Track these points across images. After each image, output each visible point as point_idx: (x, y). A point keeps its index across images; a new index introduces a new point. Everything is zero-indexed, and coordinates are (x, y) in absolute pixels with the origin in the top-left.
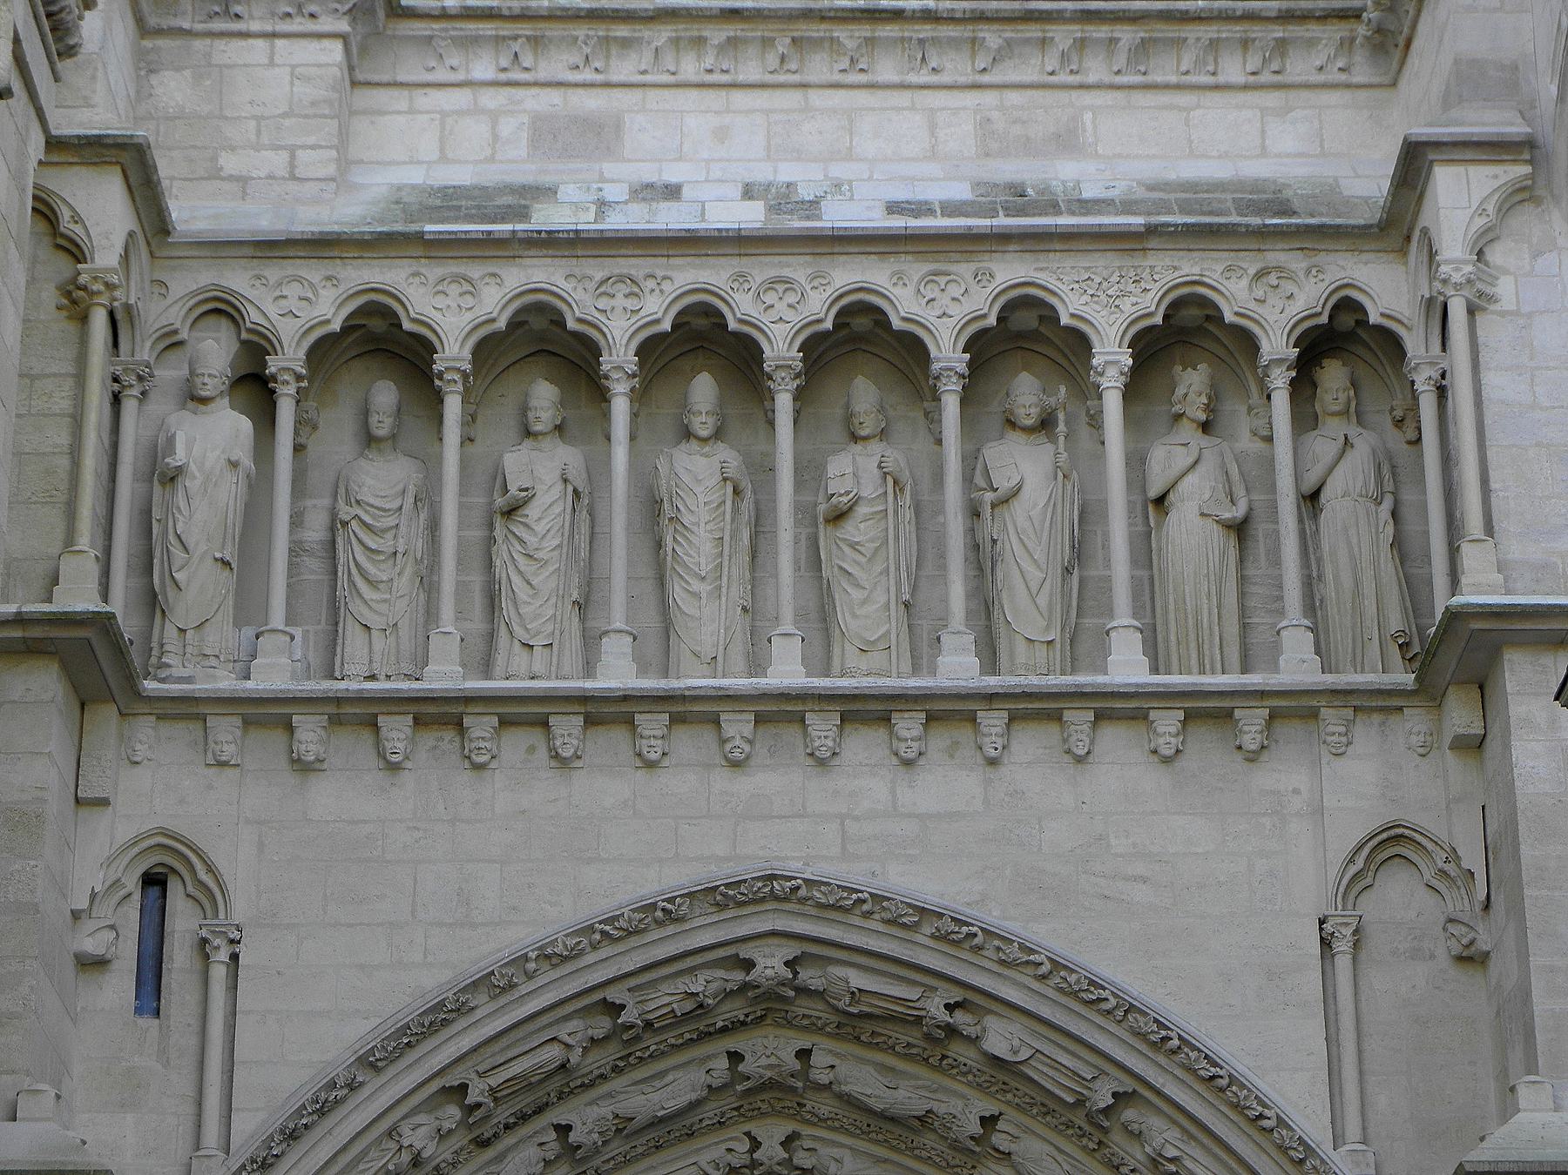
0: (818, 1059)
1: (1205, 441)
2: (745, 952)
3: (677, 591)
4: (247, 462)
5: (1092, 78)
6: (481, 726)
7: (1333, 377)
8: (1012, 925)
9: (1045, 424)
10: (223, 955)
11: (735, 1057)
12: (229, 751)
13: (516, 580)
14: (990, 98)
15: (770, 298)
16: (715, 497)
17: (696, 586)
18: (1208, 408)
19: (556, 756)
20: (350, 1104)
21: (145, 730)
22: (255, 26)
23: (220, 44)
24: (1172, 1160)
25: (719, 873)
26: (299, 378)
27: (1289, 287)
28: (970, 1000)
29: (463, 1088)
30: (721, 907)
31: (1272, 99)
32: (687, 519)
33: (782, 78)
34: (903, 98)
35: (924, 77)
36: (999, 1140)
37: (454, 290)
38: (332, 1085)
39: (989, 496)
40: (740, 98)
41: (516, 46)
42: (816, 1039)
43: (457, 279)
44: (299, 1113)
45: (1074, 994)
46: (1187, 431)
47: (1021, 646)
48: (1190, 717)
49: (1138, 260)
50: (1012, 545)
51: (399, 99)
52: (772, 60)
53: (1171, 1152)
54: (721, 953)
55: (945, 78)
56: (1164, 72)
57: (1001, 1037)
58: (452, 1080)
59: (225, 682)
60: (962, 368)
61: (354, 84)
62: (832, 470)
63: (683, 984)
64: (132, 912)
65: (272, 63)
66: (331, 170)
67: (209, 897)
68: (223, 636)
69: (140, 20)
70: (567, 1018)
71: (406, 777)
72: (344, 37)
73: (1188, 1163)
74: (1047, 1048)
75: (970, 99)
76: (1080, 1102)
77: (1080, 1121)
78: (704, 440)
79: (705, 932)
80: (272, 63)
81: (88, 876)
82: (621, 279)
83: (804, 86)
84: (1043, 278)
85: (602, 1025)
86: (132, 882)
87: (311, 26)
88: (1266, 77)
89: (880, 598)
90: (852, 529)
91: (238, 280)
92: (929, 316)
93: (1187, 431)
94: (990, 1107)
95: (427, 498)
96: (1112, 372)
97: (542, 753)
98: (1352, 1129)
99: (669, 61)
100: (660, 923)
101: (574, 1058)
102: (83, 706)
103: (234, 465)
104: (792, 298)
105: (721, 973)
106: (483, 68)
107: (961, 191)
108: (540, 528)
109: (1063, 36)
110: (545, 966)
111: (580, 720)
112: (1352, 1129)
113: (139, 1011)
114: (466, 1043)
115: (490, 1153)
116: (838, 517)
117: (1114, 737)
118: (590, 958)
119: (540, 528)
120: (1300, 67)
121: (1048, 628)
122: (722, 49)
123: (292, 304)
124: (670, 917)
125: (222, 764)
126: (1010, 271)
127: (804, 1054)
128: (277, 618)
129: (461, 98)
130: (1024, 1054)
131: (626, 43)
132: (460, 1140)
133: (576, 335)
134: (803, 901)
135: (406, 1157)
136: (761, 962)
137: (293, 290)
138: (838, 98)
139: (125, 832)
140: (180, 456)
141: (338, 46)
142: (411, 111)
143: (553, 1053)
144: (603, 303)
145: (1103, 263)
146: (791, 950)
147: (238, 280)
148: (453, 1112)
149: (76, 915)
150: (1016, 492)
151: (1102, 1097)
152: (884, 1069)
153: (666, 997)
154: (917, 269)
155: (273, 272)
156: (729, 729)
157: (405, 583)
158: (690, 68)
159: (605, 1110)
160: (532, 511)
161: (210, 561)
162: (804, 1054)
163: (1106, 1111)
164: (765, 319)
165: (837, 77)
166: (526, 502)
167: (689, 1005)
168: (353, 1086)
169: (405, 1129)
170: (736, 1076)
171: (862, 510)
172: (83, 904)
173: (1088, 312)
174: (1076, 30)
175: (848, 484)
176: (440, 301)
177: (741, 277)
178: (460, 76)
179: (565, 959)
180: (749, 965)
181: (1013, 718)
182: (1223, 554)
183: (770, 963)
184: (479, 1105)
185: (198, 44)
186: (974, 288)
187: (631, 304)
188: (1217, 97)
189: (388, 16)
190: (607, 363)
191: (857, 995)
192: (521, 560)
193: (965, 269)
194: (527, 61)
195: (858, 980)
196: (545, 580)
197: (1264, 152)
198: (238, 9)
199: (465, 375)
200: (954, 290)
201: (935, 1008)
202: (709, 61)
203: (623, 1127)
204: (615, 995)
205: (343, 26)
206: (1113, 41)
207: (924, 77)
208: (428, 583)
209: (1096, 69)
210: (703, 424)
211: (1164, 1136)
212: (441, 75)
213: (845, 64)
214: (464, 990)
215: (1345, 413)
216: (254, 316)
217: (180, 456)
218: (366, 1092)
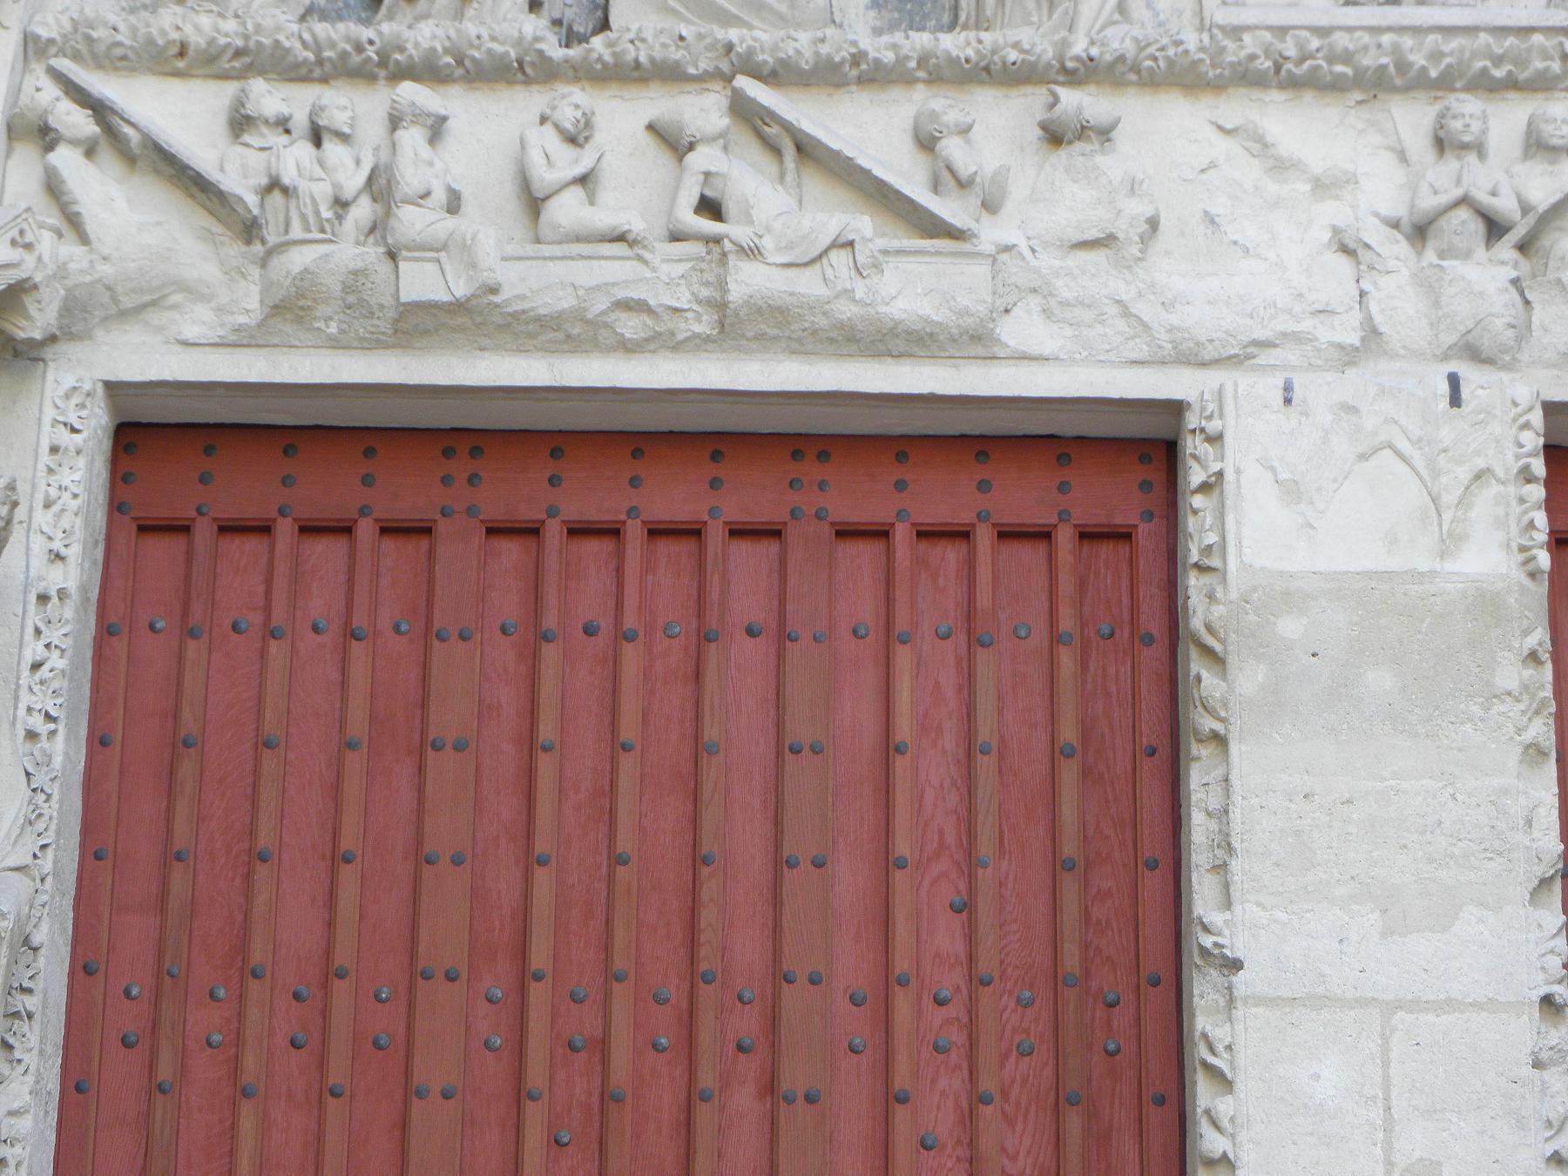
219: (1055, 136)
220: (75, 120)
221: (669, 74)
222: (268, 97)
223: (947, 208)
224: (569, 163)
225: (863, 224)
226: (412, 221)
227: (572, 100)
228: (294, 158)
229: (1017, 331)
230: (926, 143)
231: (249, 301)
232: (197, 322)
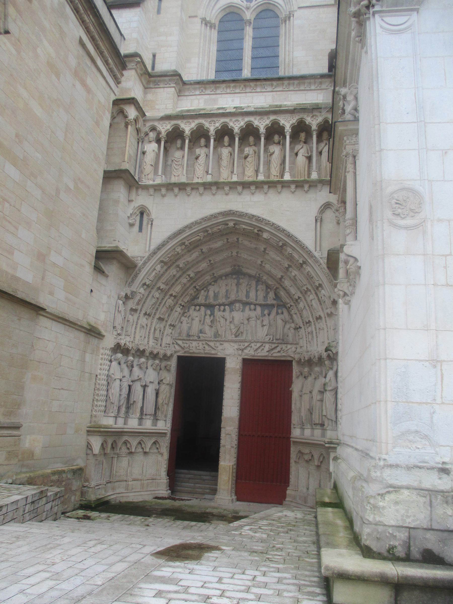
0: (240, 239)
1: (304, 145)
2: (227, 223)
3: (221, 170)
4: (156, 150)
5: (290, 89)
6: (189, 189)
7: (325, 135)
8: (268, 218)
9: (279, 143)
10: (150, 223)
11: (227, 239)
12: (152, 193)
13: (197, 168)
14: (274, 93)
15: (235, 123)
16: (227, 155)
17: (224, 168)
18: (305, 139)
19: (200, 193)
20: (168, 244)
21: (140, 191)
22: (161, 86)
23: (157, 89)
24: (291, 254)
25: (223, 210)
26: (165, 138)
27: (317, 118)
29: (185, 242)
31: (319, 91)
32: (223, 158)
33: (242, 91)
34: (261, 94)
35: (264, 90)
36: (267, 252)
37: (188, 124)
38: (164, 242)
39: (269, 154)
40: (236, 95)
41: (202, 89)
43: (188, 122)
44: (159, 246)
46: (302, 144)
47: (273, 176)
48: (297, 187)
49: (293, 115)
50: (272, 161)
51: (185, 98)
52: (241, 89)
53: (290, 252)
54: (224, 223)
55: (268, 90)
56: (302, 88)
57: (265, 235)
58: (183, 241)
59: (151, 183)
60: (264, 133)
61: (178, 96)
62: (245, 150)
64: (138, 218)
65: (164, 91)
66: (172, 107)
67: (148, 215)
68: (151, 176)
69: (144, 86)
70: (201, 232)
71: (178, 197)
74: (272, 237)
75: (271, 93)
76: (278, 245)
78: (226, 147)
80: (164, 91)
81: (130, 211)
82: (213, 121)
83: (246, 93)
84: (279, 118)
85: (206, 234)
86: (138, 213)
87: (170, 86)
88: (318, 88)
89: (251, 169)
90: (248, 159)
91: (156, 124)
92: (260, 125)
93: (302, 144)
94: (265, 247)
95: (183, 157)
96: (288, 132)
97: (198, 193)
98: (318, 249)
99: (225, 89)
101: (202, 238)
102: (130, 186)
103: (154, 151)
104: (239, 123)
105: (223, 226)
106: (197, 93)
107: (268, 106)
108: (201, 160)
109: (286, 82)
111: (203, 188)
112: (318, 249)
113: (139, 232)
114: (185, 236)
115: (191, 253)
116: (246, 158)
117: (285, 190)
119: (201, 160)
120: (324, 86)
121: (277, 173)
122: (233, 87)
123: (164, 127)
124: (215, 217)
125: (151, 195)
126: (272, 117)
127: (238, 239)
128: (160, 173)
129: (194, 97)
130: (269, 238)
131: (219, 87)
132: (186, 251)
133: (206, 130)
135: (176, 253)
136: (229, 224)
137: (164, 125)
138: (250, 94)
139: (137, 205)
140: (145, 149)
142: (187, 99)
143: (198, 237)
144: (210, 125)
145: (288, 116)
146: (234, 222)
147: (156, 124)
148: (183, 247)
149: (129, 217)
150: (273, 153)
151: (281, 244)
152: (250, 241)
153: (215, 229)
154: (258, 118)
155: (161, 122)
156: (225, 189)
157: (181, 169)
158: (228, 91)
159: (208, 247)
160: (200, 158)
161: (149, 165)
162: (238, 239)
163: (281, 246)
164: (234, 126)
165: (251, 91)
166: (199, 156)
167: (219, 231)
168: (168, 242)
169: (176, 248)
170: (228, 242)
171: (249, 156)
172: (129, 215)
173: (285, 123)
174: (287, 82)
175: (247, 152)
176: (186, 126)
177: (231, 120)
178: (194, 94)
180: (227, 224)
181: (269, 187)
182: (306, 161)
184: (187, 245)
185: (153, 90)
186: (267, 120)
187: (214, 125)
188: (311, 92)
189: (183, 85)
190: (210, 134)
191: (244, 229)
192: (198, 165)
193: (265, 117)
194: (204, 91)
195: (244, 226)
196: (201, 168)
197: (317, 100)
198: (159, 84)
200: (264, 121)
201: (256, 231)
202: (231, 90)
203: (210, 249)
205: (174, 85)
206: (294, 84)
207: (264, 90)
208: (183, 168)
209: (291, 88)
210: (226, 144)
211: (289, 250)
212: (191, 94)
213: (252, 89)
214: (184, 228)
215: (327, 140)
216: (158, 129)
217: (145, 149)
218: (170, 242)
219: (221, 344)
220: (175, 343)
221: (202, 341)
222: (184, 342)
223: (215, 348)
224: (198, 345)
225: (211, 349)
226: (190, 348)
227: (198, 342)
228: (185, 345)
229: (219, 354)
230: (215, 344)
231: (183, 352)
232: (181, 352)
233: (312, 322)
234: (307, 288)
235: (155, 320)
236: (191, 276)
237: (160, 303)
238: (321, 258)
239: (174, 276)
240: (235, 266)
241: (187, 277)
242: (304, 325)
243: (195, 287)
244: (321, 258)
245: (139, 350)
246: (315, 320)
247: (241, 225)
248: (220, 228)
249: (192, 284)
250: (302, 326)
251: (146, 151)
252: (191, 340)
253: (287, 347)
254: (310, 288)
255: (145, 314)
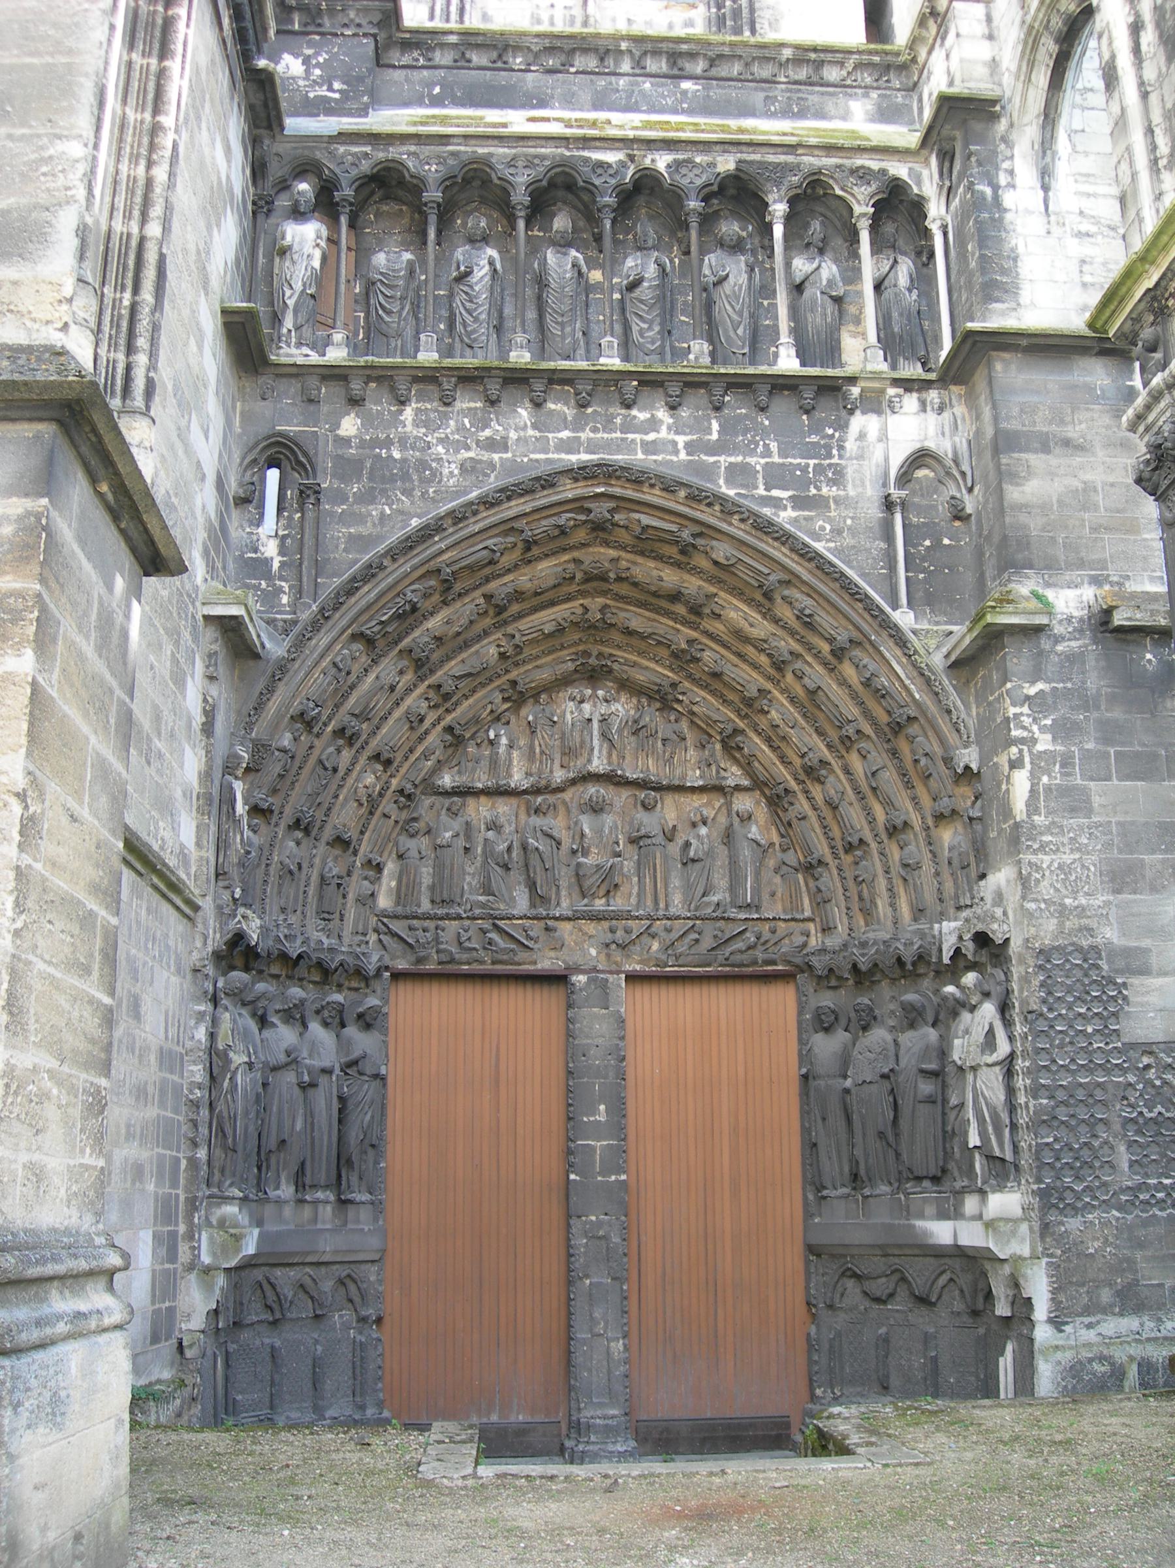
26: (351, 204)
28: (706, 530)
30: (576, 480)
42: (623, 554)
45: (761, 529)
57: (722, 551)
63: (552, 521)
72: (374, 36)
73: (817, 618)
77: (758, 597)
79: (569, 490)
100: (543, 488)
110: (482, 508)
118: (506, 505)
134: (618, 478)
141: (371, 41)
167: (556, 532)
168: (381, 567)
179: (492, 505)
180: (590, 511)
183: (601, 510)
191: (646, 528)
195: (646, 520)
199: (439, 205)
201: (686, 535)
203: (518, 595)
204: (521, 524)
233: (874, 845)
234: (858, 732)
235: (322, 848)
236: (443, 691)
237: (340, 787)
238: (914, 632)
239: (392, 688)
240: (586, 654)
241: (431, 694)
242: (836, 856)
243: (449, 729)
244: (914, 632)
245: (284, 956)
246: (884, 836)
247: (636, 516)
248: (562, 522)
249: (439, 720)
250: (829, 858)
251: (290, 247)
252: (441, 919)
253: (773, 932)
254: (868, 729)
255: (297, 824)
